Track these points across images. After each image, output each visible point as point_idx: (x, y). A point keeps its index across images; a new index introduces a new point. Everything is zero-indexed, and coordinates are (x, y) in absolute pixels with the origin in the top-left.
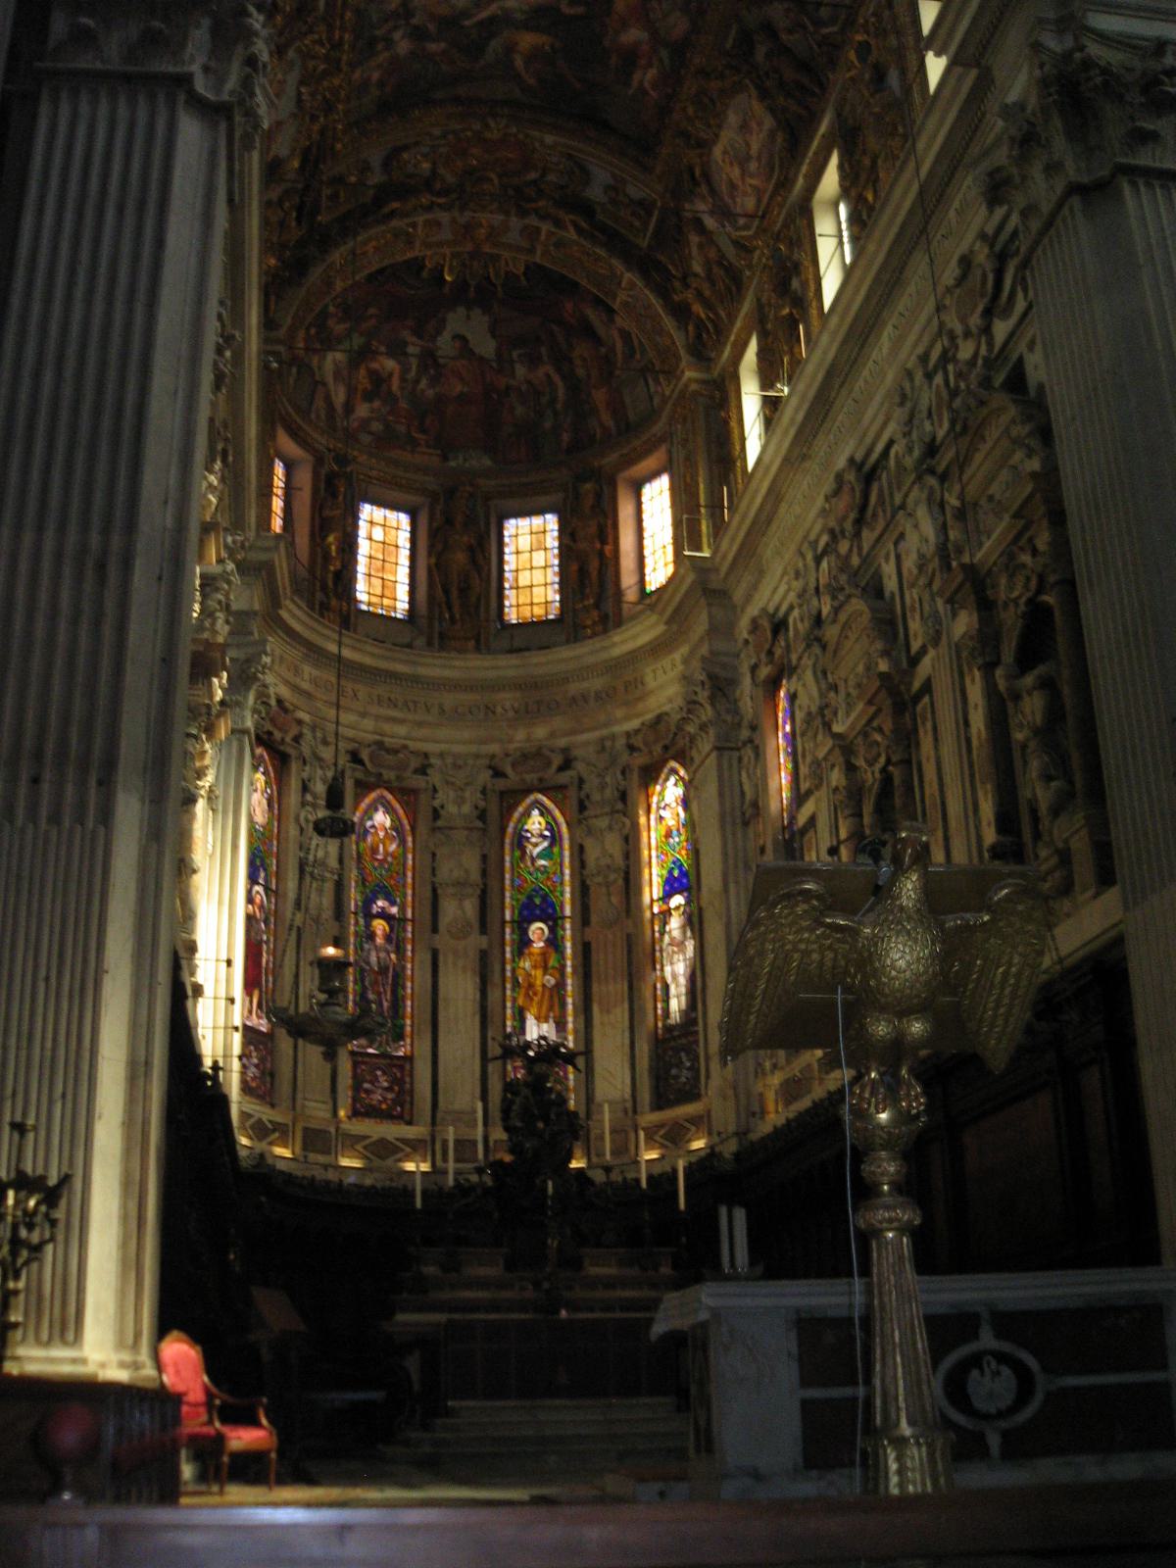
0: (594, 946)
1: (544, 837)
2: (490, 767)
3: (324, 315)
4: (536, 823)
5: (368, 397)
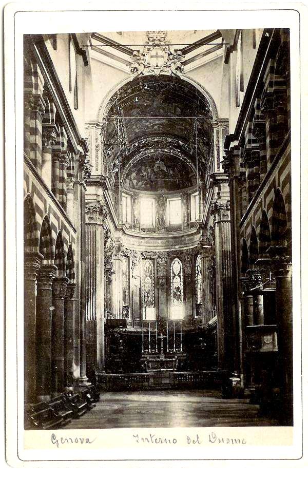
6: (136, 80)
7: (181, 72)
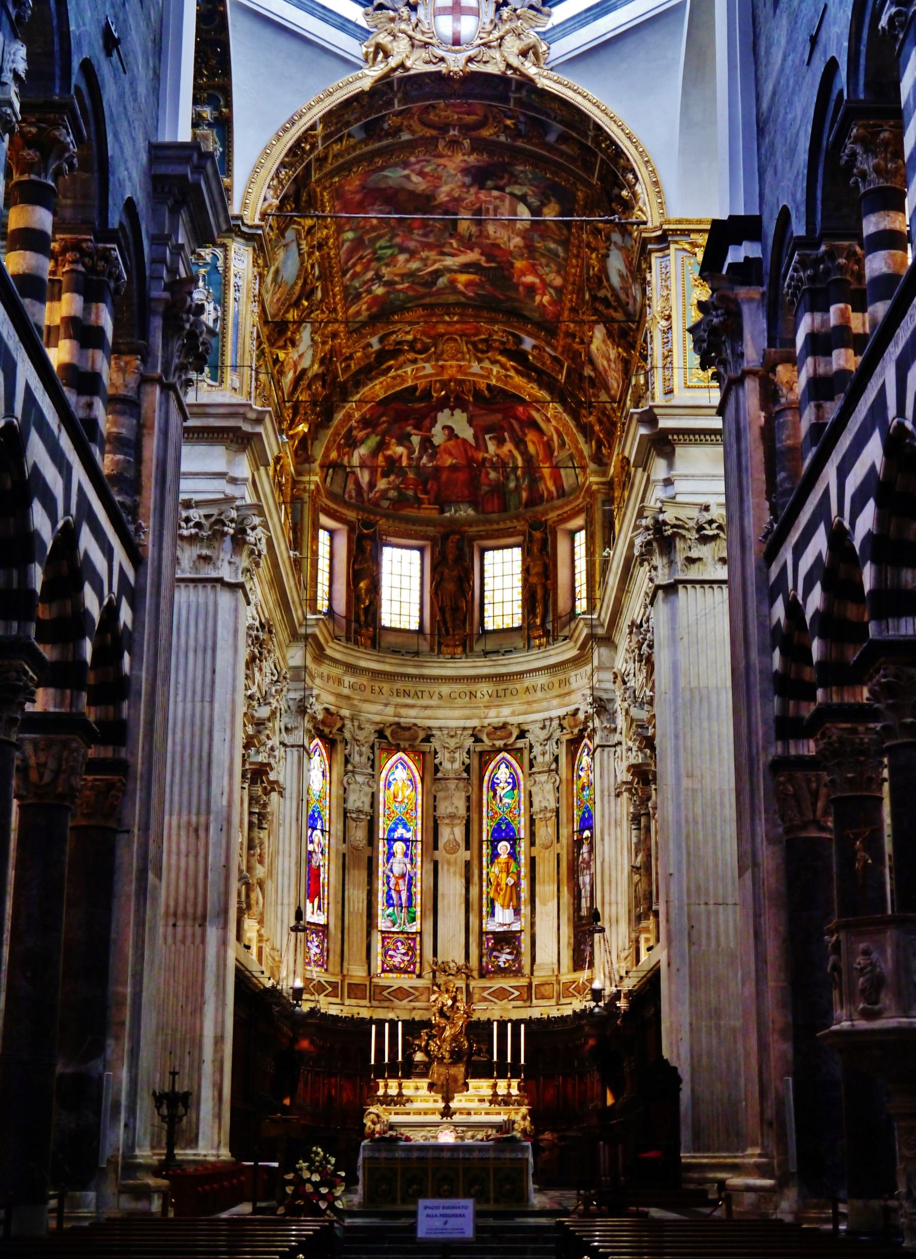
0: (537, 860)
2: (472, 735)
3: (351, 429)
4: (503, 774)
5: (385, 475)
6: (384, 84)
7: (536, 64)
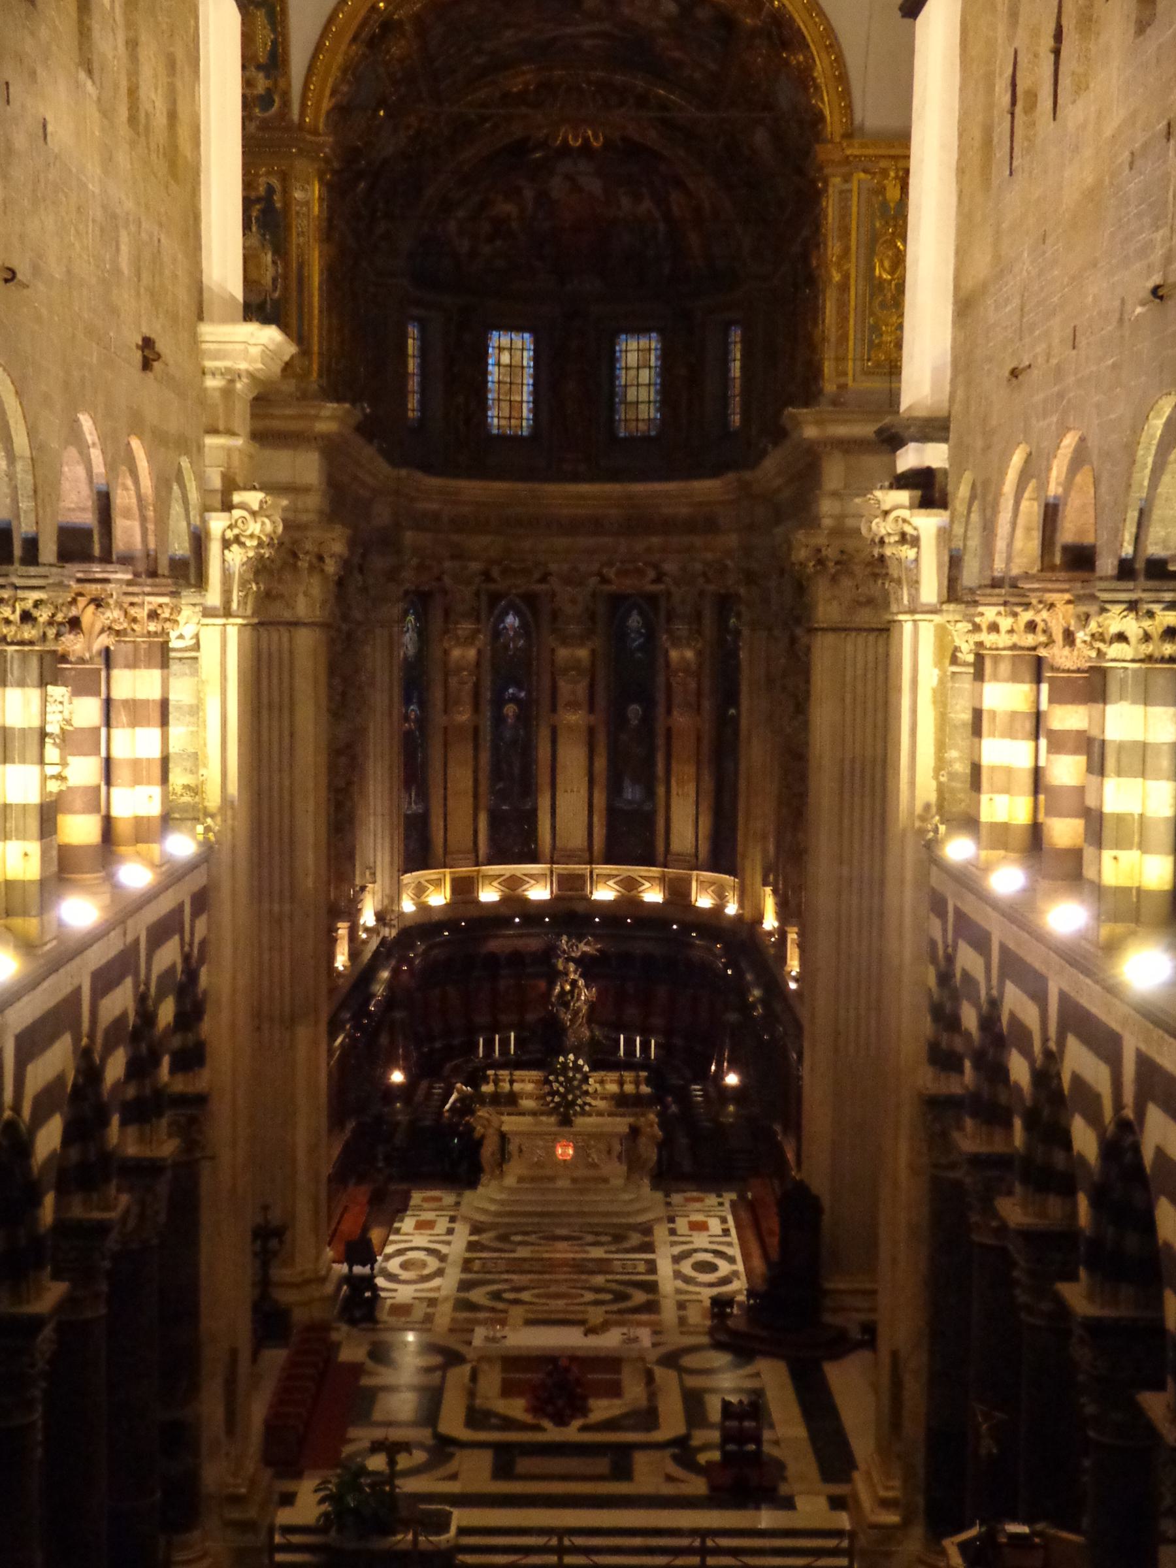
1: (641, 634)
